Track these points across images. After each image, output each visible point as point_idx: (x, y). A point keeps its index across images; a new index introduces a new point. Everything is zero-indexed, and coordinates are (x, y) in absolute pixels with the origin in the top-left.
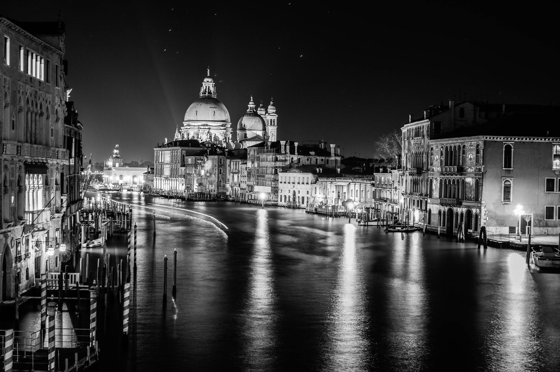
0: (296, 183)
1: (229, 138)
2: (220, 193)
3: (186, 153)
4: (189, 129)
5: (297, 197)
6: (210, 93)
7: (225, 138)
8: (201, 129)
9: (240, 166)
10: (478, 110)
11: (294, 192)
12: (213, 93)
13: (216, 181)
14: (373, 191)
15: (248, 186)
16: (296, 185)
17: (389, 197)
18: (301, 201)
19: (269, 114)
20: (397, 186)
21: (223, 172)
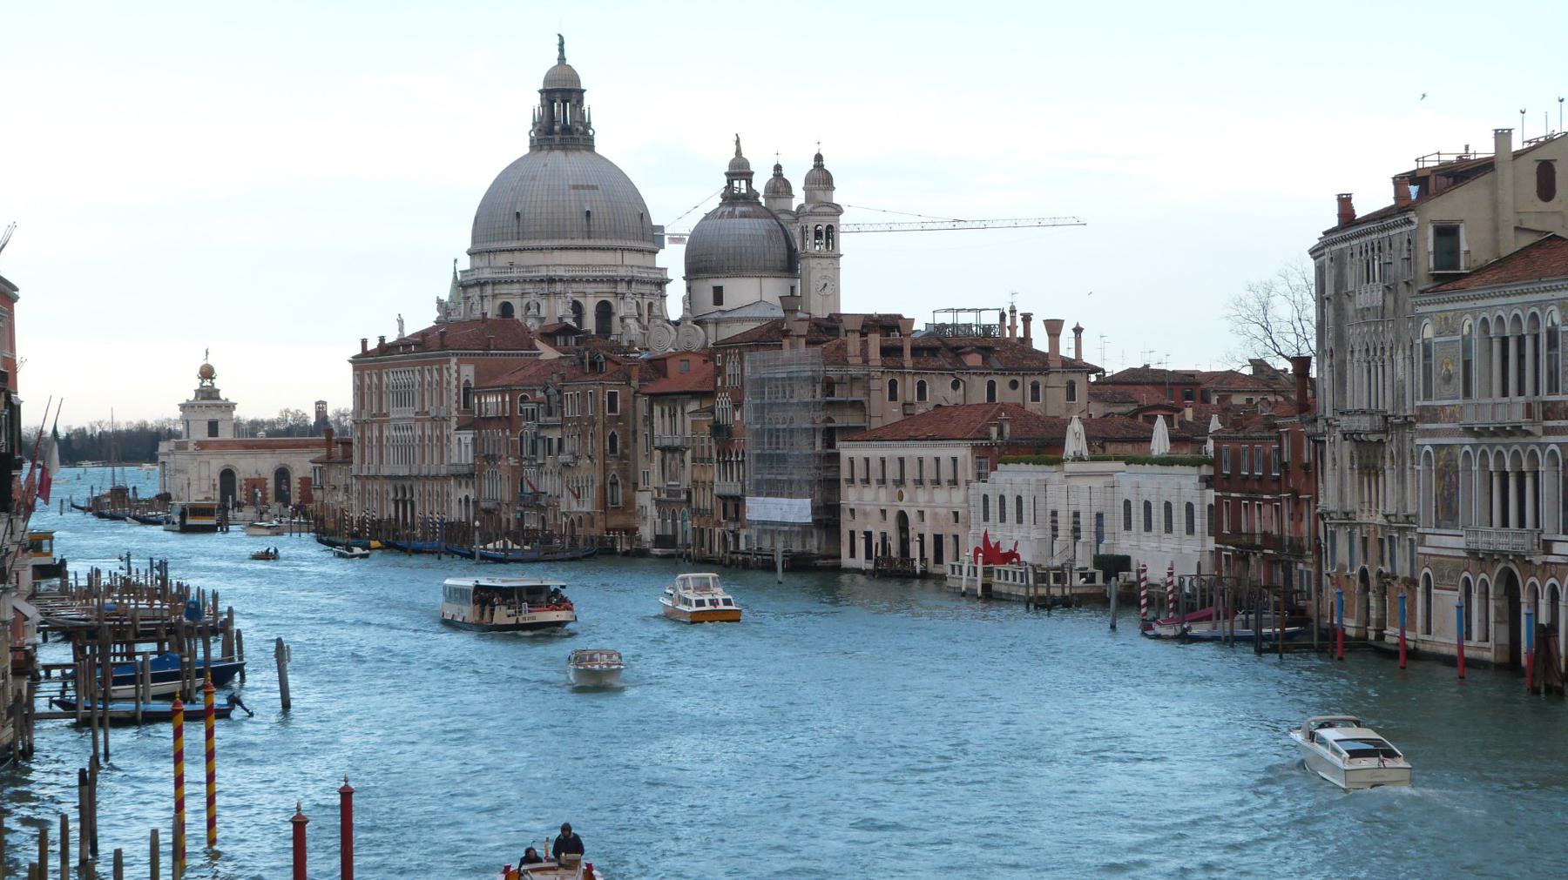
2: (612, 529)
3: (477, 374)
9: (688, 420)
11: (902, 518)
12: (581, 128)
13: (597, 484)
14: (1210, 506)
15: (724, 498)
17: (1275, 532)
18: (930, 553)
21: (626, 445)
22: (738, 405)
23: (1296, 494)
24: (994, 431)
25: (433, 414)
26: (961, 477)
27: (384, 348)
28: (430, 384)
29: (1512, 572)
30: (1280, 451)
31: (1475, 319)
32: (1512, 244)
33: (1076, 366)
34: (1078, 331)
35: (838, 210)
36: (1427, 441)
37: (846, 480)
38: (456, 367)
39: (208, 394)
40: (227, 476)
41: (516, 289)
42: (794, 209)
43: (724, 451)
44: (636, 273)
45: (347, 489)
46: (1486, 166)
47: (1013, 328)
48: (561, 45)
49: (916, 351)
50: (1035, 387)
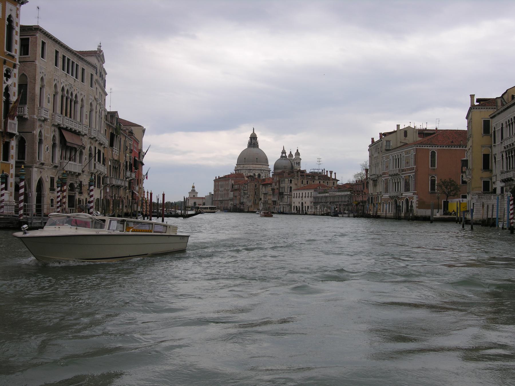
0: (304, 197)
11: (302, 203)
13: (253, 200)
15: (273, 201)
21: (258, 193)
22: (276, 185)
23: (365, 193)
24: (318, 188)
27: (219, 178)
29: (396, 200)
32: (399, 145)
33: (335, 179)
34: (335, 173)
35: (301, 159)
36: (384, 178)
39: (193, 191)
40: (195, 203)
41: (244, 171)
42: (293, 158)
43: (273, 193)
44: (265, 169)
47: (324, 173)
48: (254, 129)
50: (327, 182)
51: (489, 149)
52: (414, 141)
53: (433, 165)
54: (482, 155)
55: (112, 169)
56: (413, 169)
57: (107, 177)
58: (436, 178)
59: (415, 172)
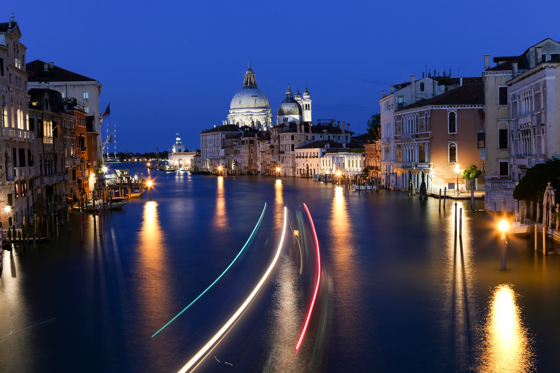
1: (269, 122)
4: (234, 116)
5: (310, 169)
6: (251, 83)
7: (266, 123)
8: (244, 115)
10: (437, 84)
16: (309, 158)
17: (375, 166)
19: (304, 99)
20: (380, 155)
21: (254, 151)
22: (275, 141)
24: (325, 146)
25: (216, 145)
26: (319, 156)
28: (216, 139)
30: (376, 148)
31: (404, 117)
34: (349, 125)
37: (296, 157)
38: (221, 135)
43: (273, 151)
45: (200, 162)
46: (410, 83)
49: (312, 130)
51: (507, 123)
52: (433, 95)
53: (452, 129)
54: (499, 131)
55: (43, 165)
56: (428, 135)
57: (36, 178)
58: (457, 146)
59: (430, 139)
